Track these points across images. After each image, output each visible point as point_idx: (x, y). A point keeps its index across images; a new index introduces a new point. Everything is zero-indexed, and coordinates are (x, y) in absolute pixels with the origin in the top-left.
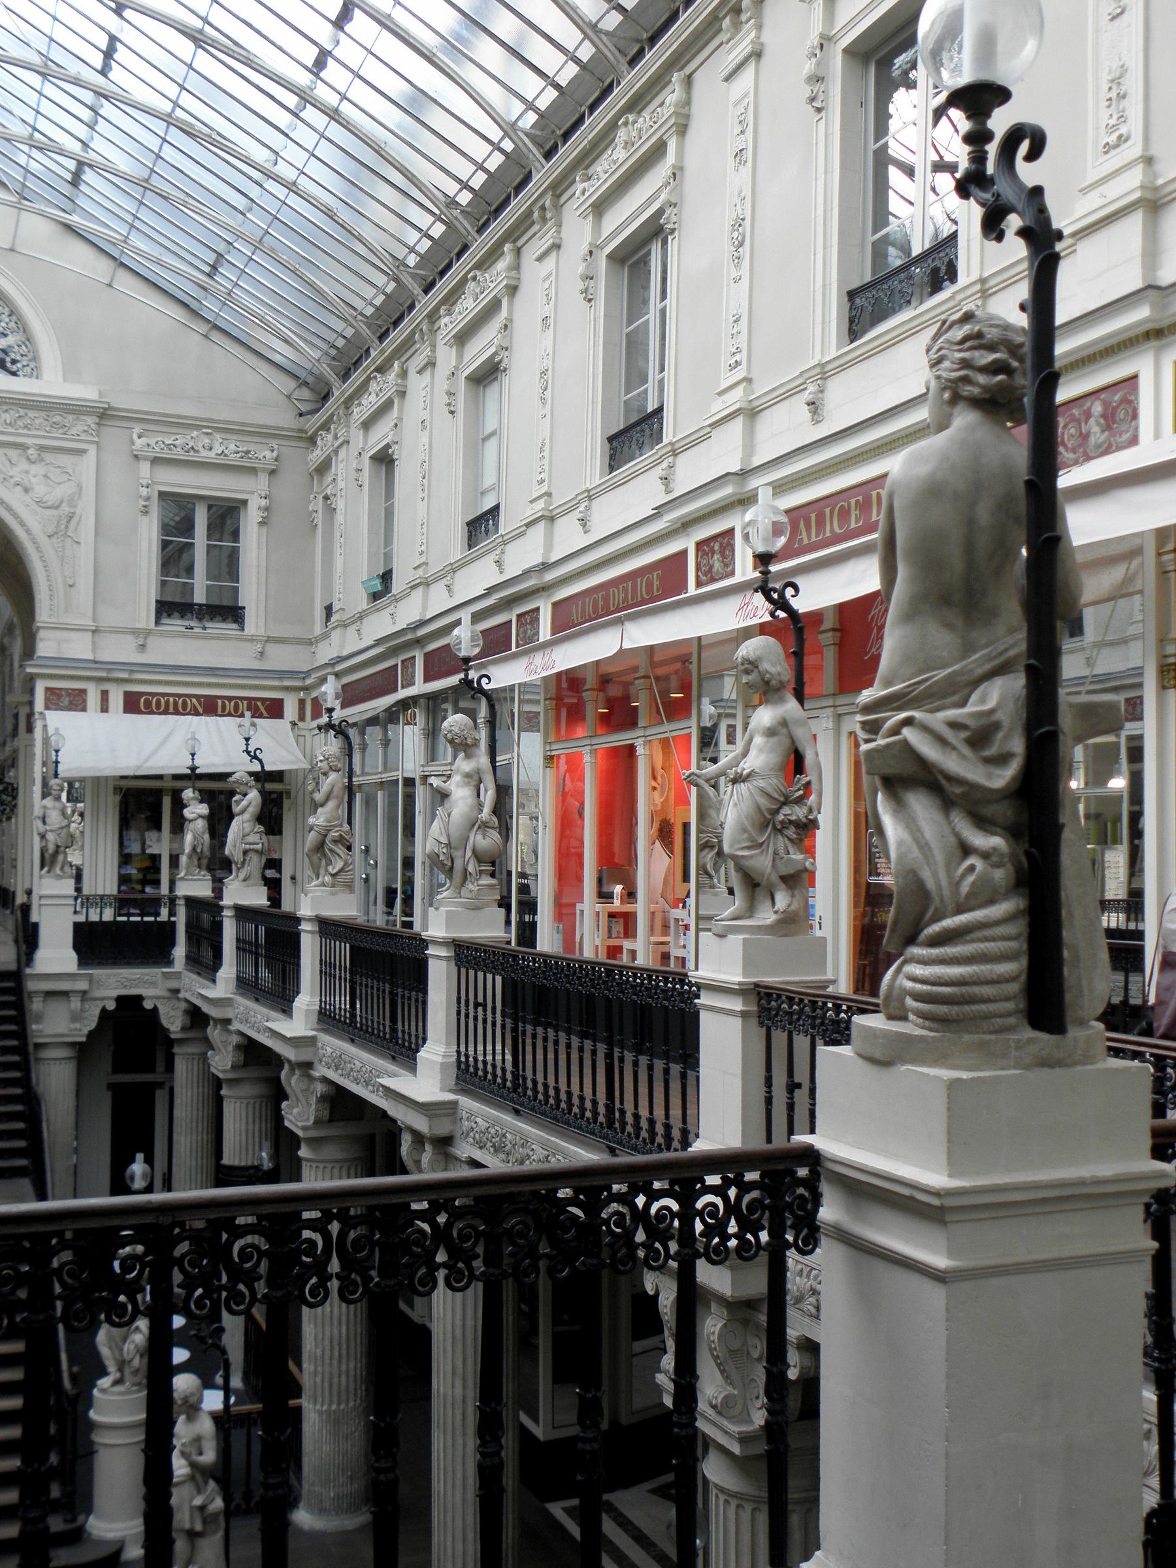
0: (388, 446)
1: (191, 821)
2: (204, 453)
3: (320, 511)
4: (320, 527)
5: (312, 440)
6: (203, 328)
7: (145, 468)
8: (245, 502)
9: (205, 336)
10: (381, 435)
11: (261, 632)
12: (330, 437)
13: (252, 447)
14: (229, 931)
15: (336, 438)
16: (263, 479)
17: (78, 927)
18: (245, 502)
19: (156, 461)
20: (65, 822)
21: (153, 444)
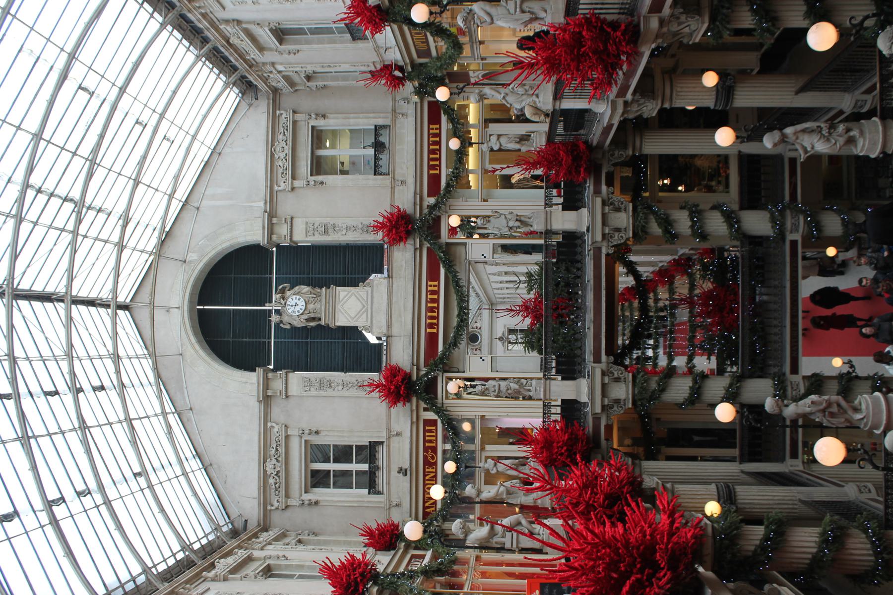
0: (271, 30)
1: (501, 145)
2: (286, 151)
3: (316, 83)
4: (325, 83)
5: (275, 91)
6: (216, 156)
7: (296, 183)
8: (313, 127)
9: (220, 154)
10: (265, 36)
11: (390, 116)
12: (271, 76)
13: (281, 125)
14: (568, 104)
15: (271, 72)
16: (298, 117)
17: (565, 208)
18: (313, 127)
19: (294, 178)
20: (503, 217)
21: (284, 180)
